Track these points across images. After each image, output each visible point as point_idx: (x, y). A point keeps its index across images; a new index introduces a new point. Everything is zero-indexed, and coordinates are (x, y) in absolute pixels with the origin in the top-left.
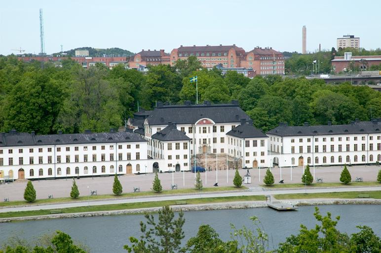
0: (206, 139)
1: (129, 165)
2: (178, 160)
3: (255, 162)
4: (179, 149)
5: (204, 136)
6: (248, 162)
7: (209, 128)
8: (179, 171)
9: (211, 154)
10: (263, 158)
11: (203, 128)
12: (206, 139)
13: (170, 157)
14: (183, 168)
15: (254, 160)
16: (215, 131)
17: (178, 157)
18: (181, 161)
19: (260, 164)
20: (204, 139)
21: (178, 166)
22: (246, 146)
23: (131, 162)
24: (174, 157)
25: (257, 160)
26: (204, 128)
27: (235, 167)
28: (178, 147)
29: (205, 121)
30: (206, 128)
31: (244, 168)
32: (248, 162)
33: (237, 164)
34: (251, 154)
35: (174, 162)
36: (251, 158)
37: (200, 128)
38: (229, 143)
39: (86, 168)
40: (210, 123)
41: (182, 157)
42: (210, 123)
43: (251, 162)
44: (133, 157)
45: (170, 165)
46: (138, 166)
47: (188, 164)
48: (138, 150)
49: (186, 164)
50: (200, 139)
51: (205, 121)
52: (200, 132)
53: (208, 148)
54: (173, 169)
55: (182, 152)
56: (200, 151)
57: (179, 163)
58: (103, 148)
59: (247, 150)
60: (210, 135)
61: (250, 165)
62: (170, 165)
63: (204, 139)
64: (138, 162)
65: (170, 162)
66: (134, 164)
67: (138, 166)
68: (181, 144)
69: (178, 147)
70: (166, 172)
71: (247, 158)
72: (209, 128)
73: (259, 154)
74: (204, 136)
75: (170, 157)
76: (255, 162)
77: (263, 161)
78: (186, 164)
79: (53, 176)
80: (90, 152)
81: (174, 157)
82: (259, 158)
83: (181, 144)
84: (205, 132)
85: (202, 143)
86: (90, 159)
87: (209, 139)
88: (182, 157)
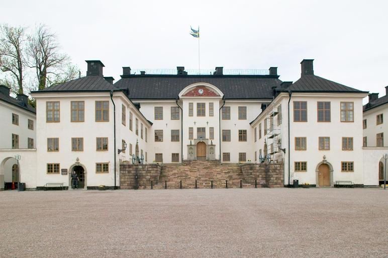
0: (204, 129)
2: (78, 154)
3: (325, 168)
5: (201, 122)
6: (301, 166)
7: (211, 105)
8: (82, 186)
9: (216, 160)
10: (347, 157)
11: (198, 104)
12: (204, 129)
14: (92, 178)
15: (320, 160)
16: (225, 114)
17: (77, 144)
18: (89, 159)
19: (339, 176)
20: (199, 129)
24: (65, 145)
25: (329, 160)
27: (263, 182)
30: (204, 105)
31: (289, 186)
32: (301, 166)
33: (267, 171)
34: (312, 144)
35: (66, 159)
36: (312, 156)
37: (191, 105)
40: (213, 94)
42: (213, 94)
43: (312, 167)
45: (53, 168)
47: (111, 168)
49: (102, 168)
50: (191, 129)
52: (191, 114)
53: (208, 149)
54: (64, 180)
56: (190, 153)
57: (82, 163)
61: (308, 177)
62: (53, 168)
63: (199, 129)
65: (53, 158)
70: (39, 189)
71: (297, 156)
73: (336, 144)
74: (201, 122)
75: (53, 145)
76: (325, 168)
77: (347, 167)
78: (102, 168)
81: (65, 145)
82: (336, 156)
84: (201, 113)
85: (195, 135)
87: (212, 129)
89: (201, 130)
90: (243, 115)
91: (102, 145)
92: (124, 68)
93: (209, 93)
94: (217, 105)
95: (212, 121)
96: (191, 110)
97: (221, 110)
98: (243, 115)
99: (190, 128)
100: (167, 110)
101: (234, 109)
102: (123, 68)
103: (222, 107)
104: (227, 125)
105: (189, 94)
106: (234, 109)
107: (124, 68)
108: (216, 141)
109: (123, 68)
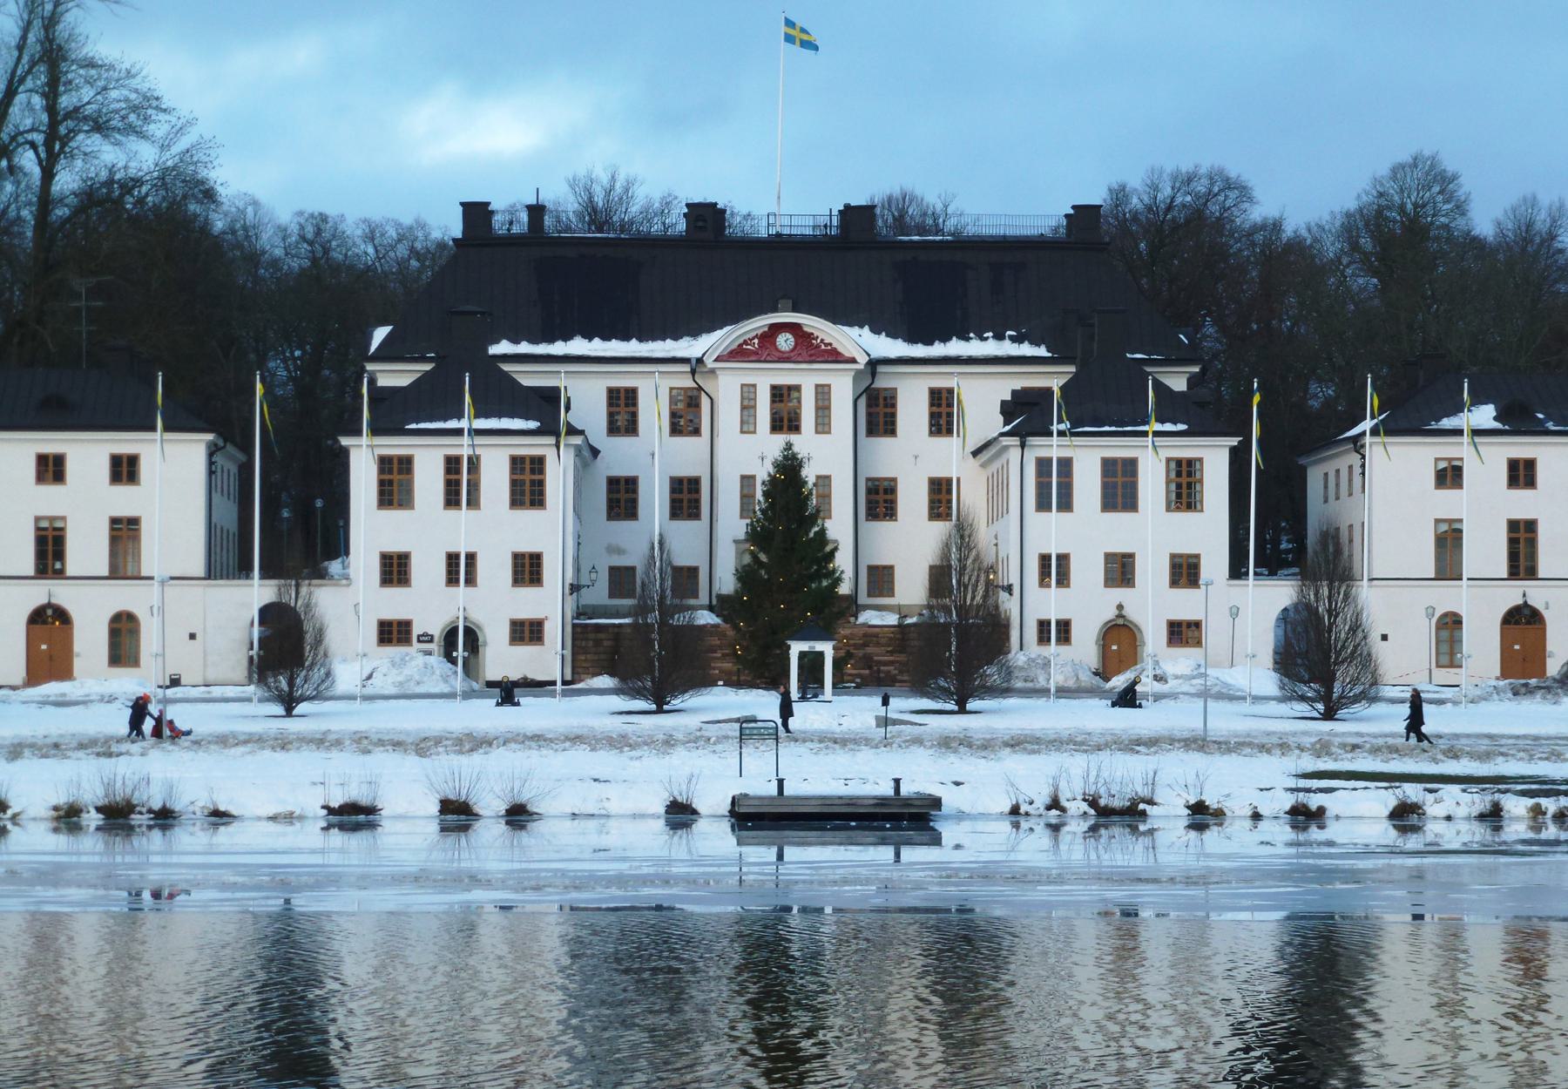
4: (473, 503)
7: (823, 392)
13: (395, 569)
18: (494, 603)
22: (1043, 505)
23: (61, 593)
24: (427, 569)
26: (781, 394)
29: (785, 341)
37: (748, 392)
38: (958, 480)
41: (495, 570)
48: (124, 500)
51: (785, 341)
52: (747, 425)
55: (496, 529)
57: (478, 616)
59: (1049, 532)
64: (123, 596)
72: (823, 392)
91: (527, 569)
92: (467, 207)
93: (810, 350)
96: (748, 406)
97: (862, 402)
99: (743, 477)
102: (462, 204)
103: (868, 388)
104: (888, 457)
105: (738, 354)
107: (467, 207)
109: (462, 204)
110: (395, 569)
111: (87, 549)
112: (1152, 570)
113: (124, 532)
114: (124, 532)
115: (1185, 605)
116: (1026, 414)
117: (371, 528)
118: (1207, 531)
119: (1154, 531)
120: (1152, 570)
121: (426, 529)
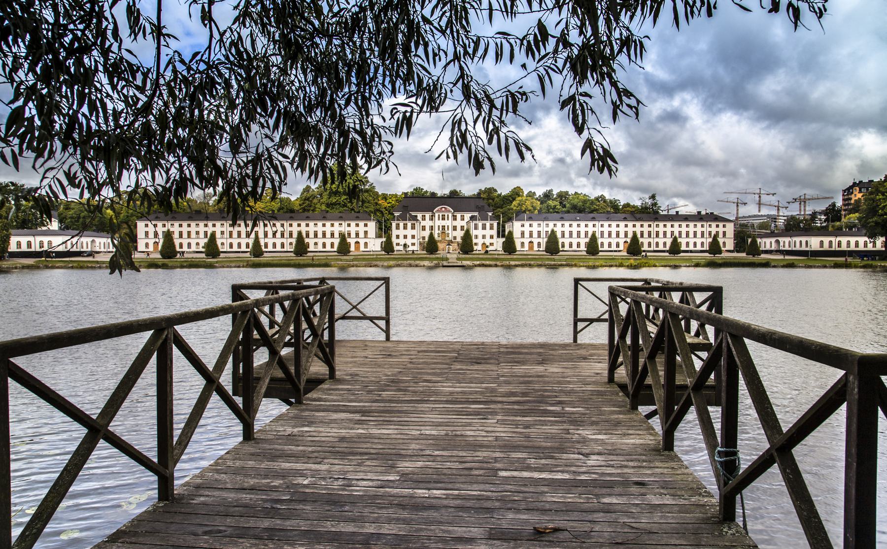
1: (357, 243)
16: (455, 218)
18: (409, 241)
21: (405, 245)
24: (401, 237)
28: (405, 228)
39: (316, 244)
41: (409, 237)
44: (362, 235)
46: (366, 244)
48: (366, 229)
49: (413, 244)
55: (409, 232)
58: (332, 225)
60: (448, 223)
66: (362, 242)
67: (366, 244)
68: (409, 225)
69: (405, 228)
78: (413, 244)
79: (285, 250)
80: (320, 229)
81: (401, 237)
83: (409, 225)
84: (443, 219)
86: (320, 235)
88: (409, 237)
89: (443, 227)
90: (463, 219)
91: (413, 237)
94: (450, 215)
95: (448, 223)
98: (463, 219)
100: (428, 215)
101: (459, 216)
104: (455, 223)
106: (459, 216)
108: (450, 232)
110: (398, 237)
111: (362, 235)
112: (488, 237)
113: (366, 232)
114: (366, 232)
115: (492, 241)
116: (472, 218)
117: (395, 232)
118: (494, 232)
119: (488, 232)
120: (488, 237)
121: (401, 232)
